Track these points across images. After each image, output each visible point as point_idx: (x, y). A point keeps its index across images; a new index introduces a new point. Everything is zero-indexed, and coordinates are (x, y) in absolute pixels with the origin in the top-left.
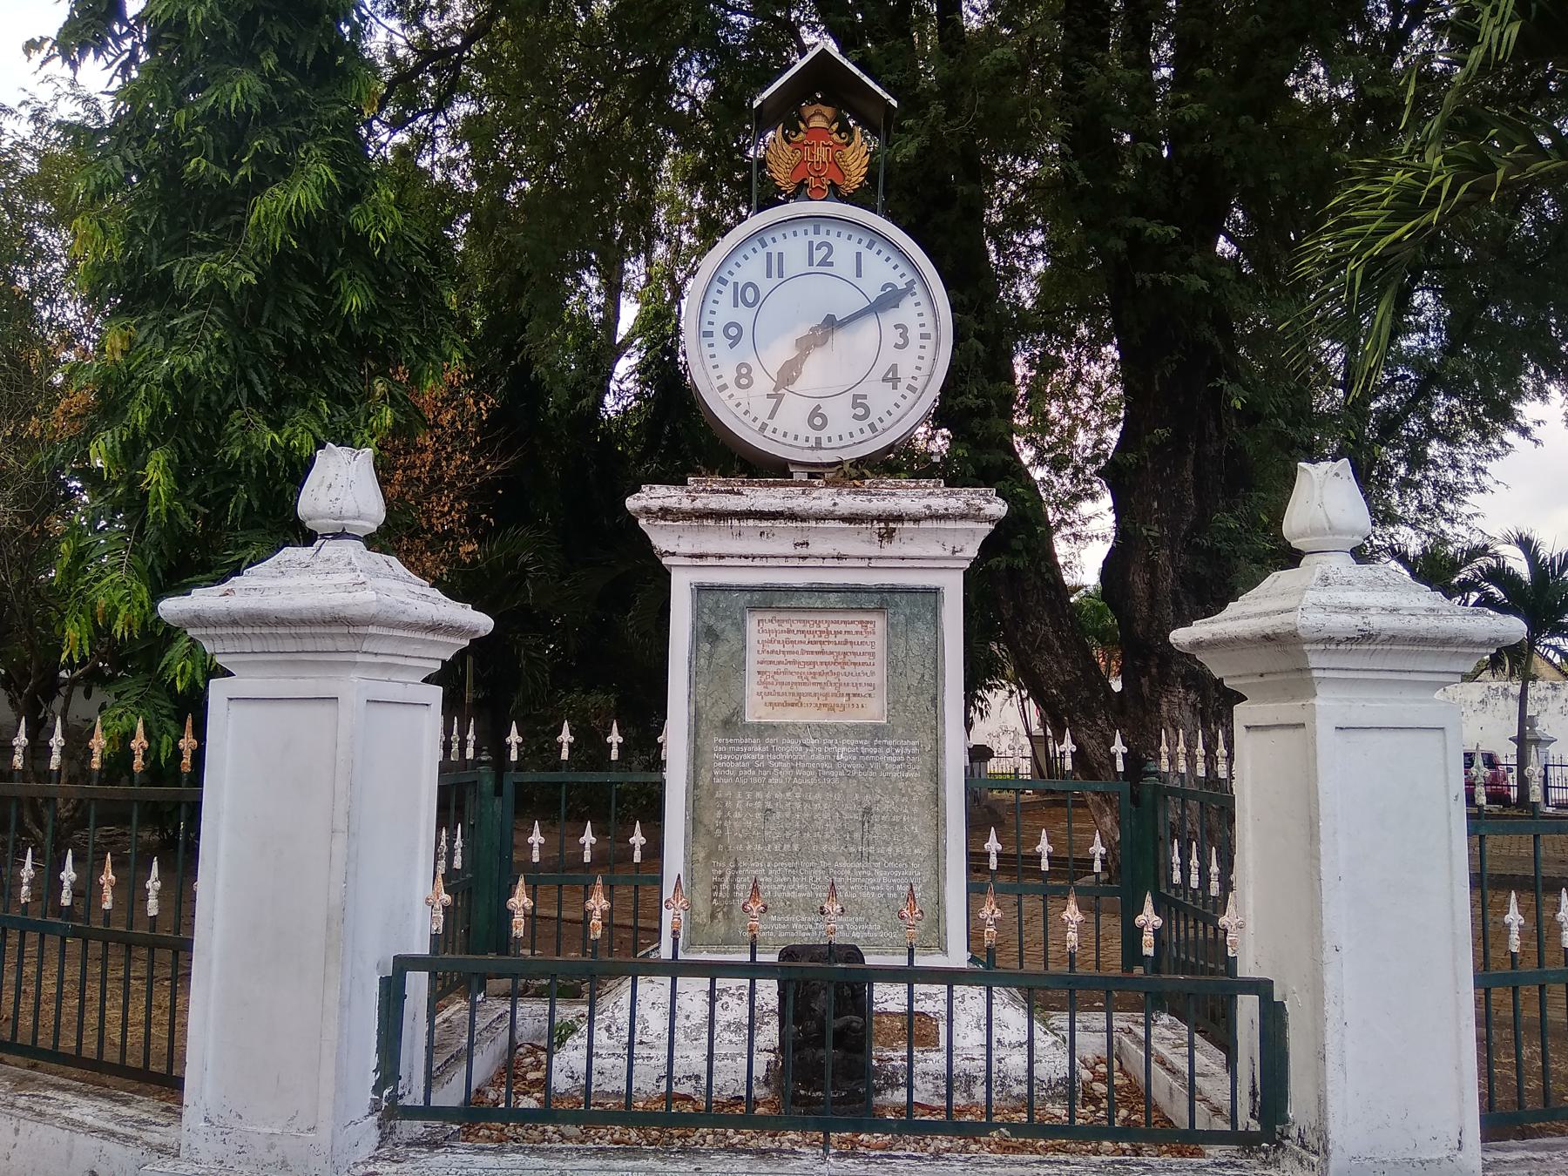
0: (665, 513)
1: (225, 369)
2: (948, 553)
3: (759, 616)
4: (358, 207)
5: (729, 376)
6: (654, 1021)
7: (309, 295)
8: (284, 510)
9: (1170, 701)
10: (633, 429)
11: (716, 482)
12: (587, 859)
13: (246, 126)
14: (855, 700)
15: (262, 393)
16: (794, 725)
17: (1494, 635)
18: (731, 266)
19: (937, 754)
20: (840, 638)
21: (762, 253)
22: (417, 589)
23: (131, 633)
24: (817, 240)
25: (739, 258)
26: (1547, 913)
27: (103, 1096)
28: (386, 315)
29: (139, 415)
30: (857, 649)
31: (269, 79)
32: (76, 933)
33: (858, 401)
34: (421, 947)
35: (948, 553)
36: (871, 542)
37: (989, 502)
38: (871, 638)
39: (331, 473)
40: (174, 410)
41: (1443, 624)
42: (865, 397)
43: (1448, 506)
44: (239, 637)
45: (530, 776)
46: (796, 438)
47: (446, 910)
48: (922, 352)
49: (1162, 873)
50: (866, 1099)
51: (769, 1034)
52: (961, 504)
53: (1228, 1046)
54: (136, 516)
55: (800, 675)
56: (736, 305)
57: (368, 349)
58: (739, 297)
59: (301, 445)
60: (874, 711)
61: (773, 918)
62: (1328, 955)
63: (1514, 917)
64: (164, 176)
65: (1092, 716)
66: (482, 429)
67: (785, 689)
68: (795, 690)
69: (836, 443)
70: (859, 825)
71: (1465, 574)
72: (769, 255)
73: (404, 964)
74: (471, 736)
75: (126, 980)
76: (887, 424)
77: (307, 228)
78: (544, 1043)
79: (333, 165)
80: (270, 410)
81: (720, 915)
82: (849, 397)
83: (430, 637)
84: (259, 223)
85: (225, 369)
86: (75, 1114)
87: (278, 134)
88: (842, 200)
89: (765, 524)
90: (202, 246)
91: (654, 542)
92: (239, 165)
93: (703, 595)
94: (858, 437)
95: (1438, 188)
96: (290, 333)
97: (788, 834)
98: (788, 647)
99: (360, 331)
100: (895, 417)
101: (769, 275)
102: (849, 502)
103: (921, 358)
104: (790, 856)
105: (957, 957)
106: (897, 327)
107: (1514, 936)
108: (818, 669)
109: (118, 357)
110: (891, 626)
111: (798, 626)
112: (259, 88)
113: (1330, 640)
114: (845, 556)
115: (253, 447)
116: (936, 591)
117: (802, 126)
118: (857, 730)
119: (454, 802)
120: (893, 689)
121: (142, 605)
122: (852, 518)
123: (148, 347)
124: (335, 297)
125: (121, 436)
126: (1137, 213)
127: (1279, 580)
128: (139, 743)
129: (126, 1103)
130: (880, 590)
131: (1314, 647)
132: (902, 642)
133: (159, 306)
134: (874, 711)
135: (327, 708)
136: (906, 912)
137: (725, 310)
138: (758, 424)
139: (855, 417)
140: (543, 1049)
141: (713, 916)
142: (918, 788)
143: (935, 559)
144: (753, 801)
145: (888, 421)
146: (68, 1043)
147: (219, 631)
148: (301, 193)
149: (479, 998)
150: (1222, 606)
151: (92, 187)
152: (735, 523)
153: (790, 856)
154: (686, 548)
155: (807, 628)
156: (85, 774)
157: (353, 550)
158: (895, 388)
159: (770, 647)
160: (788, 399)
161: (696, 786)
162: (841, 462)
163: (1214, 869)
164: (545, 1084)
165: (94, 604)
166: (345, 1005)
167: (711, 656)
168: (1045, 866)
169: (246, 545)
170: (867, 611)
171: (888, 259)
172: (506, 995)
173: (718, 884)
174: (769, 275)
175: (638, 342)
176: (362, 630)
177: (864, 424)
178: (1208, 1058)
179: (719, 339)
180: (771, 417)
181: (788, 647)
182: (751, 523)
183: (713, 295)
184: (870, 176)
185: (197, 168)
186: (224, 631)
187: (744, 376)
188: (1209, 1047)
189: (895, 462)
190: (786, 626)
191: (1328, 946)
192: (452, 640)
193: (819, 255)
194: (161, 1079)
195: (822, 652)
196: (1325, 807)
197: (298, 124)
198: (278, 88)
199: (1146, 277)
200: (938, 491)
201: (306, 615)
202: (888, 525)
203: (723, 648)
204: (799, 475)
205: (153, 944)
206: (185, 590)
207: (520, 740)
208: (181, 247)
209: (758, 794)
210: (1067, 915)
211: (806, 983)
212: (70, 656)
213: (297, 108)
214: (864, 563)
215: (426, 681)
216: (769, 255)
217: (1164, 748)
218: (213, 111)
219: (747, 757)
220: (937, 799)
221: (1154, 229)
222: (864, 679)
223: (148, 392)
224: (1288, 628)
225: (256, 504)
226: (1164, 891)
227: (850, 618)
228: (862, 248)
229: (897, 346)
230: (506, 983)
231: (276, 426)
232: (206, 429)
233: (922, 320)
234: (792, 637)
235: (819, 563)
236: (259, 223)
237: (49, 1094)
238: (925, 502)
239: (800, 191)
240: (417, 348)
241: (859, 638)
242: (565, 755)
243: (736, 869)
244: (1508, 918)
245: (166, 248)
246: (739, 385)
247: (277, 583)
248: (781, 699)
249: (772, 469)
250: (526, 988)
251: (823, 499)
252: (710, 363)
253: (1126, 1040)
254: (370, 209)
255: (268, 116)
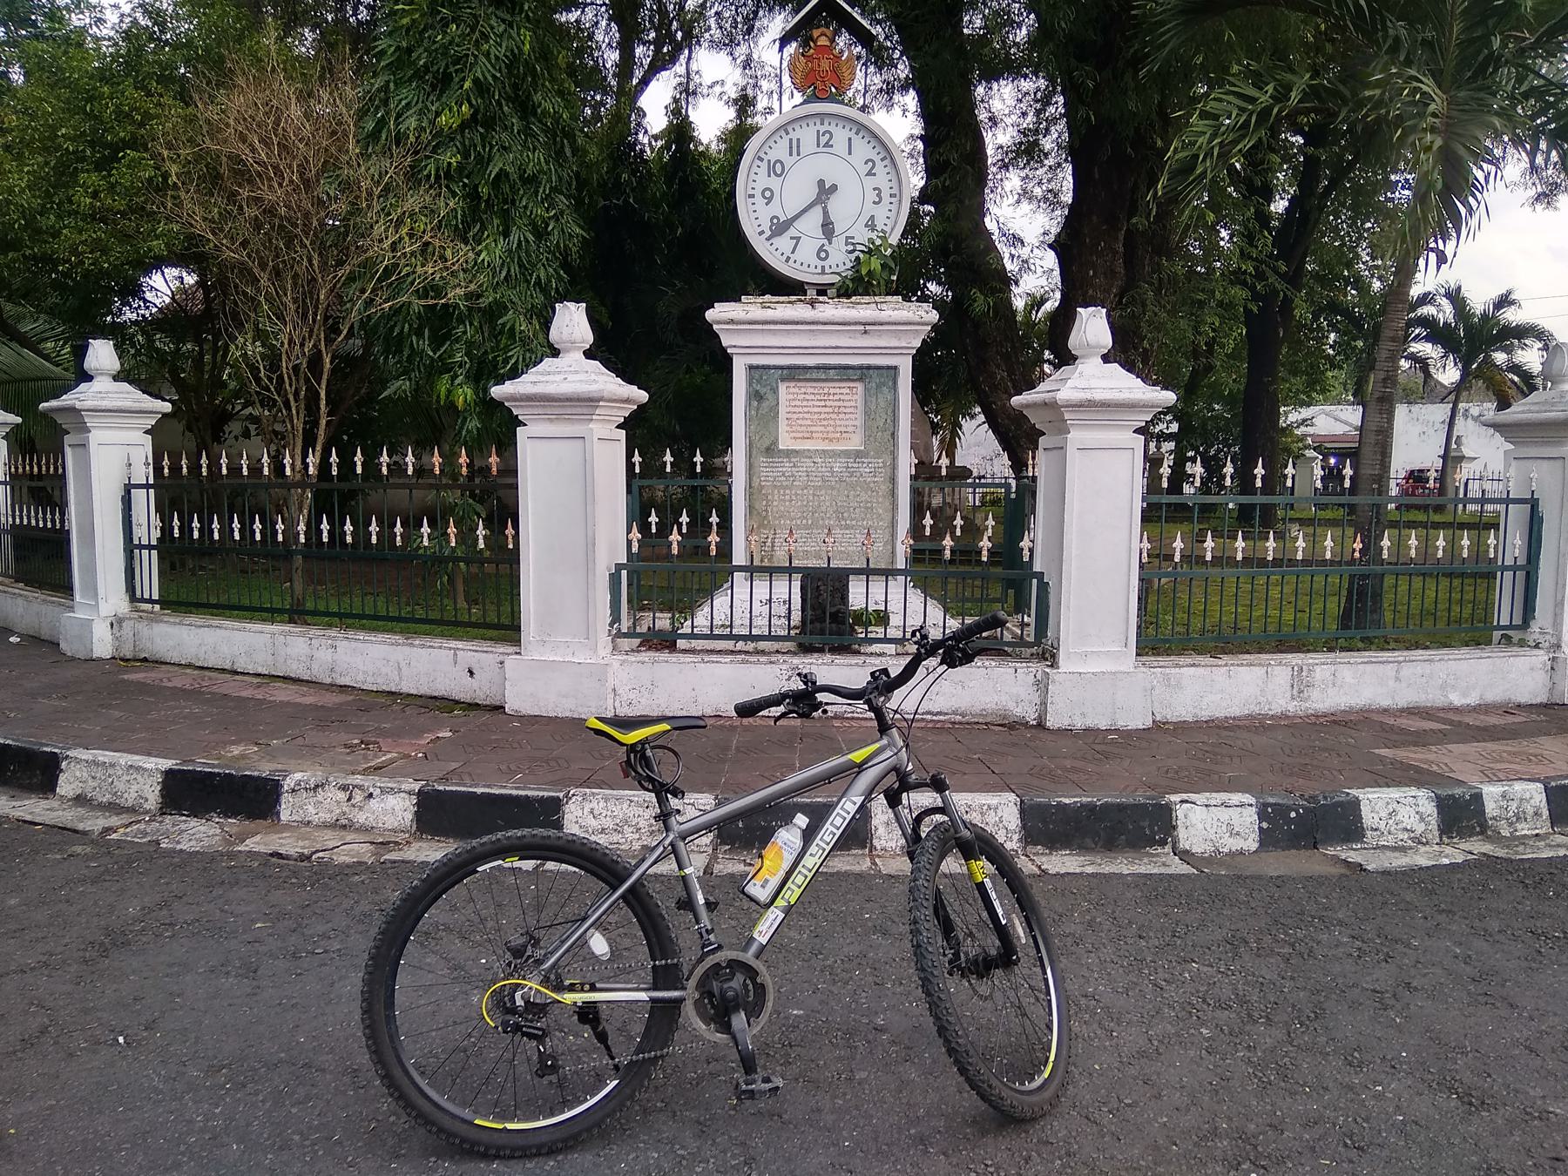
18: (766, 148)
19: (894, 467)
21: (786, 139)
24: (822, 129)
58: (771, 170)
60: (855, 443)
104: (807, 527)
116: (896, 368)
118: (846, 454)
120: (867, 428)
130: (861, 367)
134: (855, 443)
137: (763, 180)
153: (807, 527)
179: (759, 200)
183: (754, 169)
193: (823, 140)
203: (765, 404)
204: (811, 293)
220: (893, 493)
228: (852, 134)
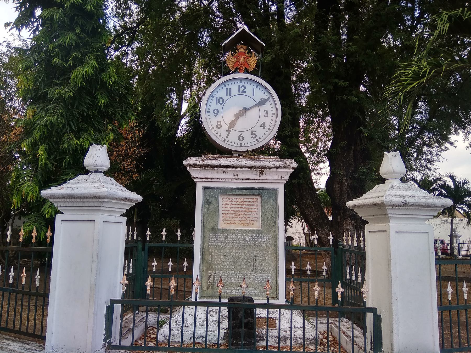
0: (195, 165)
1: (63, 121)
2: (280, 178)
3: (223, 197)
4: (104, 73)
5: (215, 125)
6: (190, 320)
7: (89, 99)
8: (80, 164)
9: (346, 223)
10: (186, 140)
11: (210, 156)
12: (170, 270)
13: (71, 49)
14: (251, 222)
15: (74, 128)
16: (233, 230)
17: (443, 204)
18: (215, 92)
19: (276, 239)
20: (247, 203)
21: (225, 88)
22: (119, 188)
23: (33, 201)
24: (241, 85)
25: (218, 90)
26: (459, 288)
27: (21, 342)
28: (112, 106)
29: (37, 135)
30: (252, 207)
31: (78, 35)
32: (14, 292)
33: (253, 133)
34: (118, 296)
35: (280, 178)
36: (257, 175)
37: (292, 163)
38: (256, 203)
39: (94, 152)
40: (48, 133)
41: (428, 201)
42: (255, 131)
43: (429, 166)
44: (65, 202)
45: (153, 245)
46: (234, 143)
47: (127, 285)
48: (272, 118)
49: (344, 276)
50: (254, 344)
51: (225, 324)
52: (283, 164)
53: (363, 328)
54: (35, 165)
55: (235, 214)
56: (217, 104)
57: (106, 116)
59: (85, 145)
60: (257, 226)
61: (226, 288)
62: (394, 300)
63: (449, 289)
64: (46, 63)
65: (323, 228)
66: (140, 140)
67: (231, 219)
68: (233, 219)
69: (246, 145)
70: (252, 260)
71: (434, 186)
72: (227, 89)
73: (114, 302)
74: (135, 232)
75: (29, 306)
76: (261, 140)
77: (88, 79)
78: (156, 326)
79: (97, 61)
80: (76, 134)
81: (210, 288)
82: (250, 131)
83: (123, 202)
84: (74, 78)
85: (63, 121)
86: (12, 348)
87: (80, 52)
88: (249, 73)
89: (225, 169)
90: (57, 84)
91: (191, 174)
92: (68, 61)
93: (206, 190)
94: (253, 143)
95: (425, 71)
96: (83, 111)
97: (231, 263)
98: (232, 206)
99: (104, 110)
100: (264, 137)
101: (227, 95)
102: (250, 163)
103: (272, 120)
104: (232, 269)
105: (282, 300)
106: (265, 111)
107: (450, 295)
108: (240, 213)
109: (31, 117)
110: (262, 200)
111: (234, 200)
112: (75, 38)
113: (394, 205)
114: (249, 179)
115: (71, 144)
116: (276, 190)
117: (237, 51)
118: (252, 231)
119: (130, 252)
120: (263, 219)
121: (36, 192)
122: (251, 168)
123: (40, 114)
124: (97, 100)
125: (31, 141)
126: (336, 78)
127: (378, 188)
128: (34, 234)
129: (28, 344)
130: (259, 189)
131: (389, 207)
132: (266, 205)
133: (43, 102)
135: (90, 224)
136: (266, 287)
137: (214, 105)
138: (223, 139)
139: (252, 137)
140: (156, 328)
141: (208, 288)
142: (271, 249)
143: (276, 180)
144: (221, 252)
145: (262, 139)
146: (10, 326)
147: (59, 200)
148: (87, 69)
149: (136, 313)
150: (362, 195)
151: (24, 67)
152: (216, 168)
153: (232, 269)
154: (201, 176)
155: (237, 200)
156: (18, 243)
157: (100, 176)
158: (264, 129)
159: (226, 206)
160: (232, 132)
161: (203, 248)
162: (248, 151)
163: (360, 274)
164: (156, 339)
165: (22, 192)
166: (95, 314)
167: (208, 209)
168: (309, 273)
169: (68, 174)
170: (256, 195)
171: (262, 91)
172: (145, 311)
173: (210, 278)
174: (227, 95)
175: (188, 114)
176: (102, 200)
177: (255, 139)
178: (358, 332)
179: (211, 113)
180: (227, 137)
181: (232, 206)
182: (221, 169)
183: (210, 101)
184: (257, 66)
185: (56, 61)
186: (61, 200)
187: (219, 125)
188: (358, 328)
189: (264, 151)
190: (231, 200)
191: (394, 298)
192: (130, 203)
193: (242, 89)
194: (39, 337)
195: (242, 208)
196: (392, 256)
197: (86, 49)
198: (80, 38)
199: (339, 97)
200: (277, 160)
201: (85, 195)
202: (262, 169)
203: (212, 206)
204: (235, 155)
205: (37, 295)
206: (49, 188)
207: (150, 234)
208: (50, 85)
209: (222, 251)
210: (315, 288)
211: (236, 308)
212: (14, 207)
213: (86, 44)
214: (255, 181)
215: (122, 215)
216: (227, 89)
217: (344, 237)
218: (61, 45)
219: (219, 239)
220: (276, 252)
221: (341, 83)
222: (254, 216)
223: (40, 128)
224: (381, 202)
225: (71, 162)
226: (344, 281)
227: (250, 197)
228: (254, 87)
229: (265, 116)
230: (145, 308)
231: (78, 138)
232: (57, 139)
233: (272, 109)
234: (233, 203)
235: (241, 181)
236: (74, 78)
237: (4, 341)
238: (273, 163)
239: (236, 70)
240: (121, 116)
241: (253, 204)
242: (164, 238)
243: (215, 273)
244: (448, 290)
245: (46, 85)
246: (217, 127)
247: (77, 186)
248: (229, 222)
249: (227, 153)
250: (151, 309)
251: (242, 161)
252: (209, 121)
253: (333, 326)
254: (107, 74)
255: (77, 46)
